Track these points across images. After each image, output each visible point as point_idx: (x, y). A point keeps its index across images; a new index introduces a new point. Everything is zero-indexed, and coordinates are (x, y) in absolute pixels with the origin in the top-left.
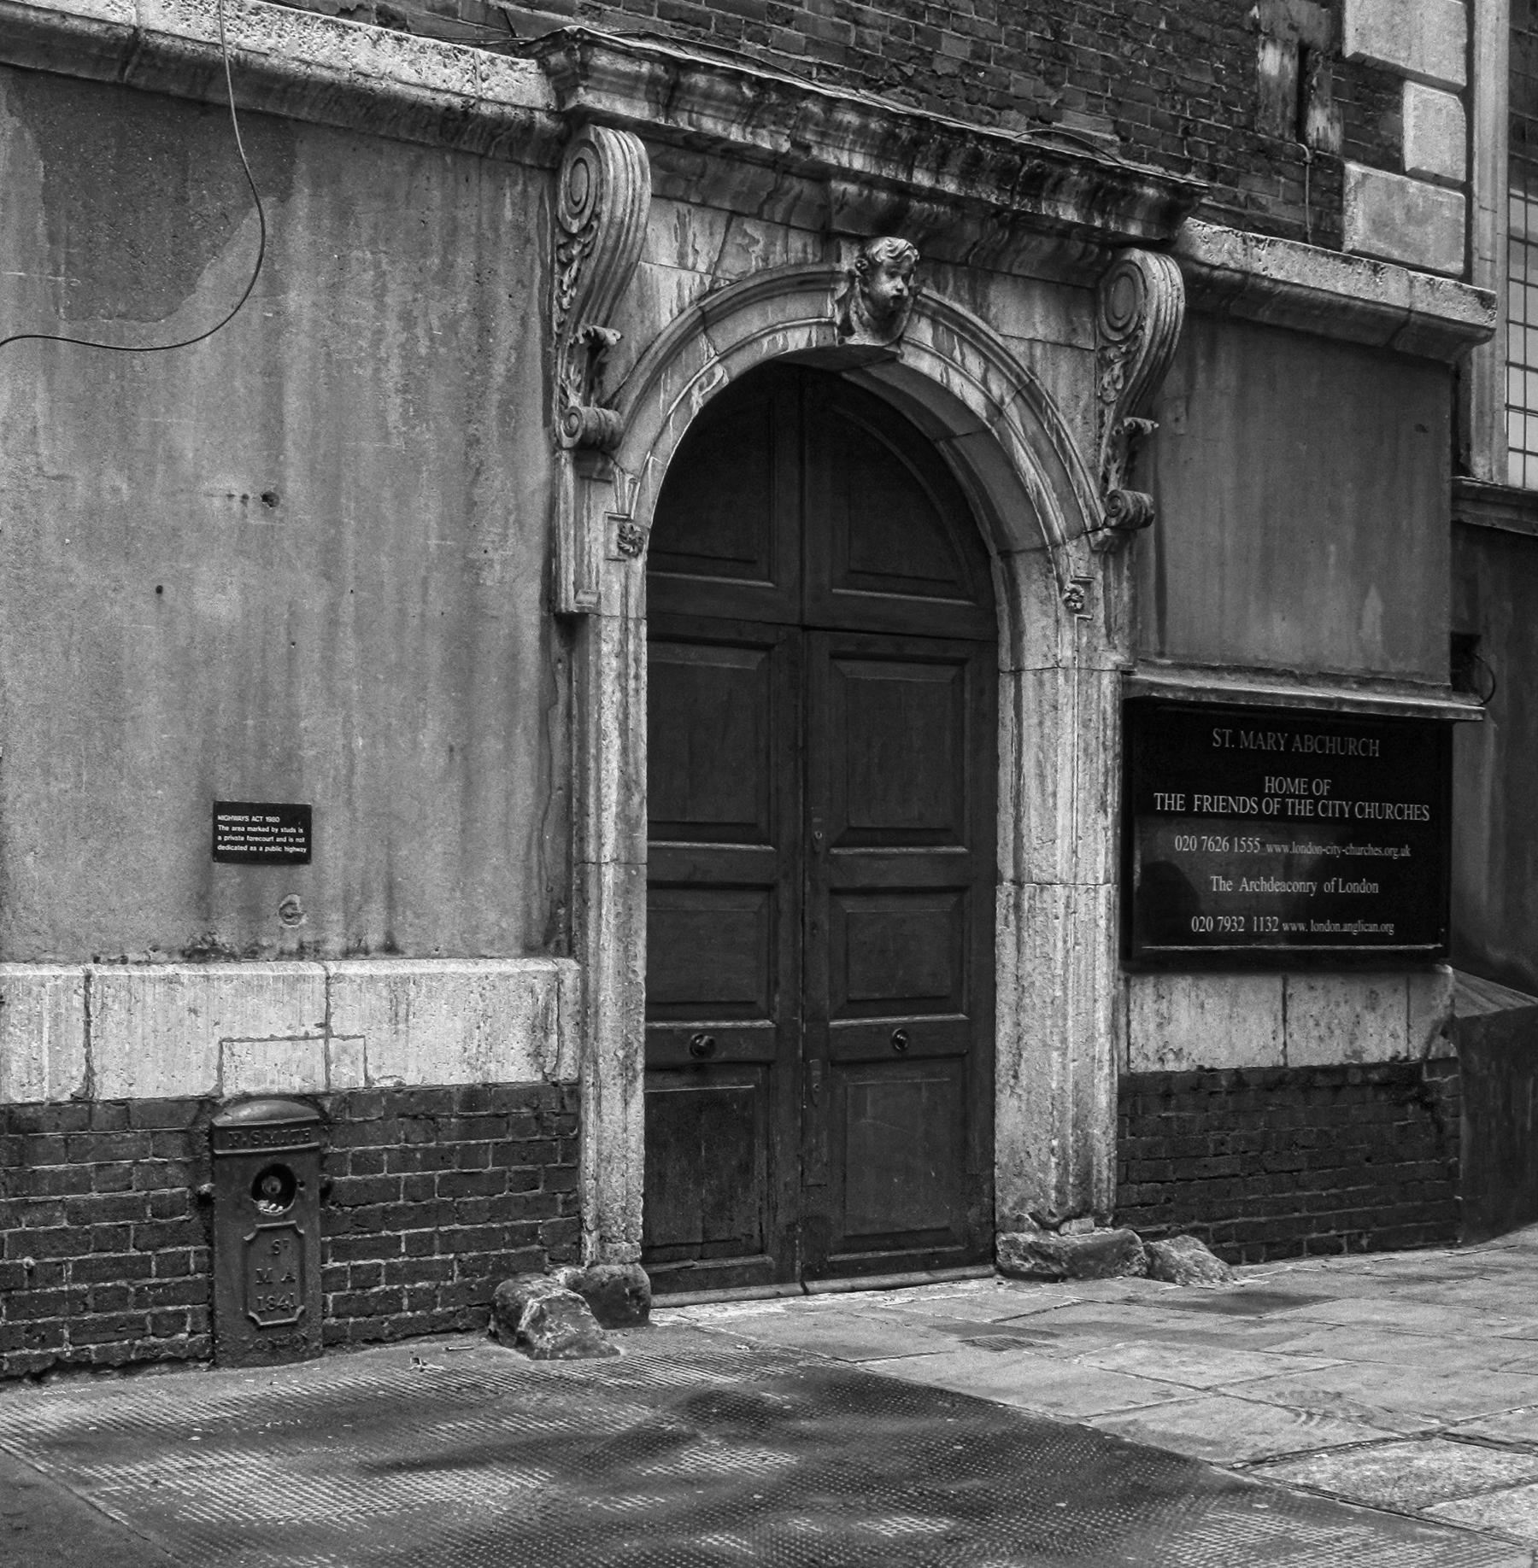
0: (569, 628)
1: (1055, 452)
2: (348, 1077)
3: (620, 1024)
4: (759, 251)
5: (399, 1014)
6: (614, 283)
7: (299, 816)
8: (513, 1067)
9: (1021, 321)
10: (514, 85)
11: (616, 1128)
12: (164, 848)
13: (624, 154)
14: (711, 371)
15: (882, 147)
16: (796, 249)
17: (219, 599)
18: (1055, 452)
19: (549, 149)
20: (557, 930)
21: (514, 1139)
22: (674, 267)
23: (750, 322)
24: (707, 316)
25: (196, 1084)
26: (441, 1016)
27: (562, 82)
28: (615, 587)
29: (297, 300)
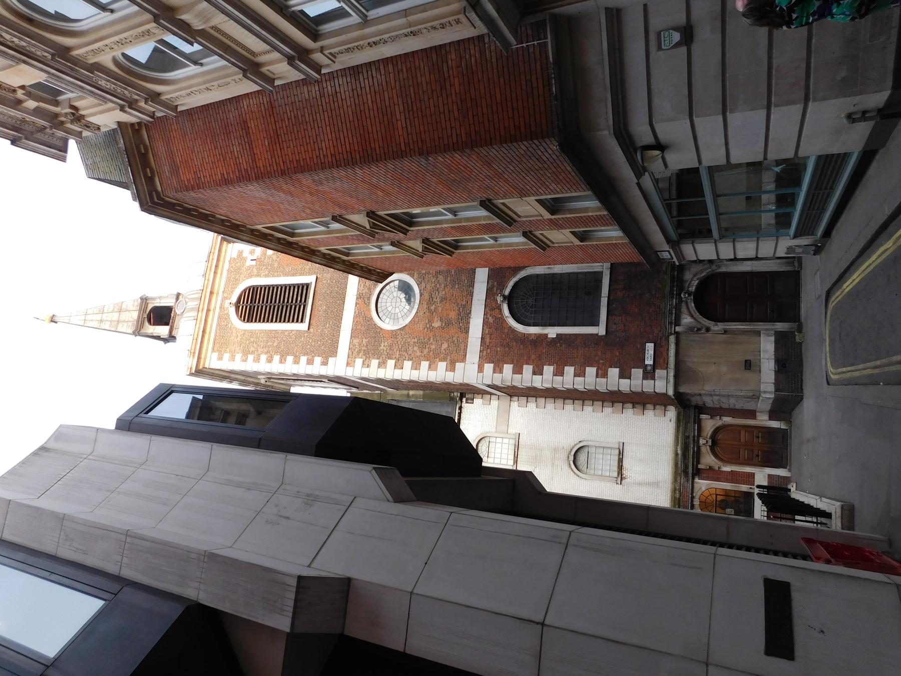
0: (725, 332)
1: (701, 272)
2: (773, 357)
3: (768, 326)
4: (684, 309)
5: (766, 351)
6: (690, 329)
7: (746, 361)
8: (773, 338)
9: (688, 276)
10: (672, 339)
11: (780, 326)
12: (749, 375)
13: (678, 329)
14: (697, 315)
15: (673, 298)
16: (683, 304)
17: (724, 369)
18: (701, 272)
19: (677, 334)
20: (758, 333)
21: (782, 340)
22: (686, 320)
23: (692, 311)
24: (692, 316)
25: (773, 373)
26: (767, 347)
27: (671, 334)
28: (721, 326)
29: (695, 360)
